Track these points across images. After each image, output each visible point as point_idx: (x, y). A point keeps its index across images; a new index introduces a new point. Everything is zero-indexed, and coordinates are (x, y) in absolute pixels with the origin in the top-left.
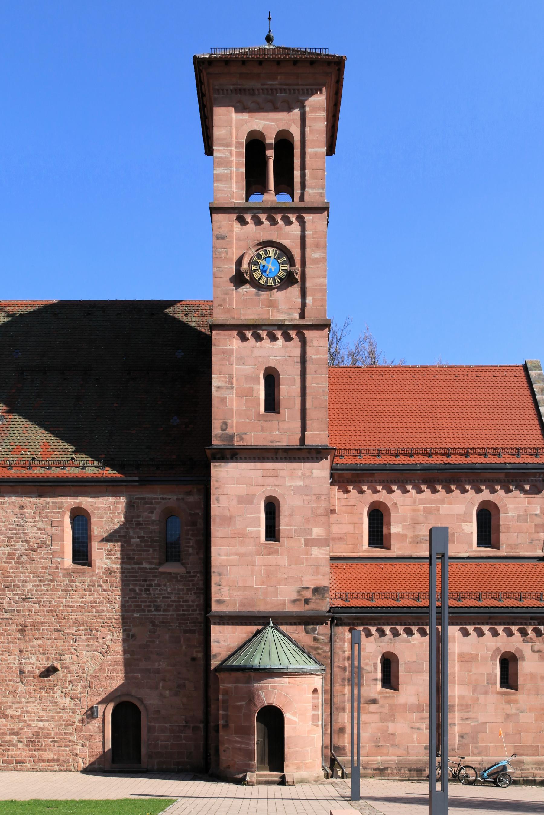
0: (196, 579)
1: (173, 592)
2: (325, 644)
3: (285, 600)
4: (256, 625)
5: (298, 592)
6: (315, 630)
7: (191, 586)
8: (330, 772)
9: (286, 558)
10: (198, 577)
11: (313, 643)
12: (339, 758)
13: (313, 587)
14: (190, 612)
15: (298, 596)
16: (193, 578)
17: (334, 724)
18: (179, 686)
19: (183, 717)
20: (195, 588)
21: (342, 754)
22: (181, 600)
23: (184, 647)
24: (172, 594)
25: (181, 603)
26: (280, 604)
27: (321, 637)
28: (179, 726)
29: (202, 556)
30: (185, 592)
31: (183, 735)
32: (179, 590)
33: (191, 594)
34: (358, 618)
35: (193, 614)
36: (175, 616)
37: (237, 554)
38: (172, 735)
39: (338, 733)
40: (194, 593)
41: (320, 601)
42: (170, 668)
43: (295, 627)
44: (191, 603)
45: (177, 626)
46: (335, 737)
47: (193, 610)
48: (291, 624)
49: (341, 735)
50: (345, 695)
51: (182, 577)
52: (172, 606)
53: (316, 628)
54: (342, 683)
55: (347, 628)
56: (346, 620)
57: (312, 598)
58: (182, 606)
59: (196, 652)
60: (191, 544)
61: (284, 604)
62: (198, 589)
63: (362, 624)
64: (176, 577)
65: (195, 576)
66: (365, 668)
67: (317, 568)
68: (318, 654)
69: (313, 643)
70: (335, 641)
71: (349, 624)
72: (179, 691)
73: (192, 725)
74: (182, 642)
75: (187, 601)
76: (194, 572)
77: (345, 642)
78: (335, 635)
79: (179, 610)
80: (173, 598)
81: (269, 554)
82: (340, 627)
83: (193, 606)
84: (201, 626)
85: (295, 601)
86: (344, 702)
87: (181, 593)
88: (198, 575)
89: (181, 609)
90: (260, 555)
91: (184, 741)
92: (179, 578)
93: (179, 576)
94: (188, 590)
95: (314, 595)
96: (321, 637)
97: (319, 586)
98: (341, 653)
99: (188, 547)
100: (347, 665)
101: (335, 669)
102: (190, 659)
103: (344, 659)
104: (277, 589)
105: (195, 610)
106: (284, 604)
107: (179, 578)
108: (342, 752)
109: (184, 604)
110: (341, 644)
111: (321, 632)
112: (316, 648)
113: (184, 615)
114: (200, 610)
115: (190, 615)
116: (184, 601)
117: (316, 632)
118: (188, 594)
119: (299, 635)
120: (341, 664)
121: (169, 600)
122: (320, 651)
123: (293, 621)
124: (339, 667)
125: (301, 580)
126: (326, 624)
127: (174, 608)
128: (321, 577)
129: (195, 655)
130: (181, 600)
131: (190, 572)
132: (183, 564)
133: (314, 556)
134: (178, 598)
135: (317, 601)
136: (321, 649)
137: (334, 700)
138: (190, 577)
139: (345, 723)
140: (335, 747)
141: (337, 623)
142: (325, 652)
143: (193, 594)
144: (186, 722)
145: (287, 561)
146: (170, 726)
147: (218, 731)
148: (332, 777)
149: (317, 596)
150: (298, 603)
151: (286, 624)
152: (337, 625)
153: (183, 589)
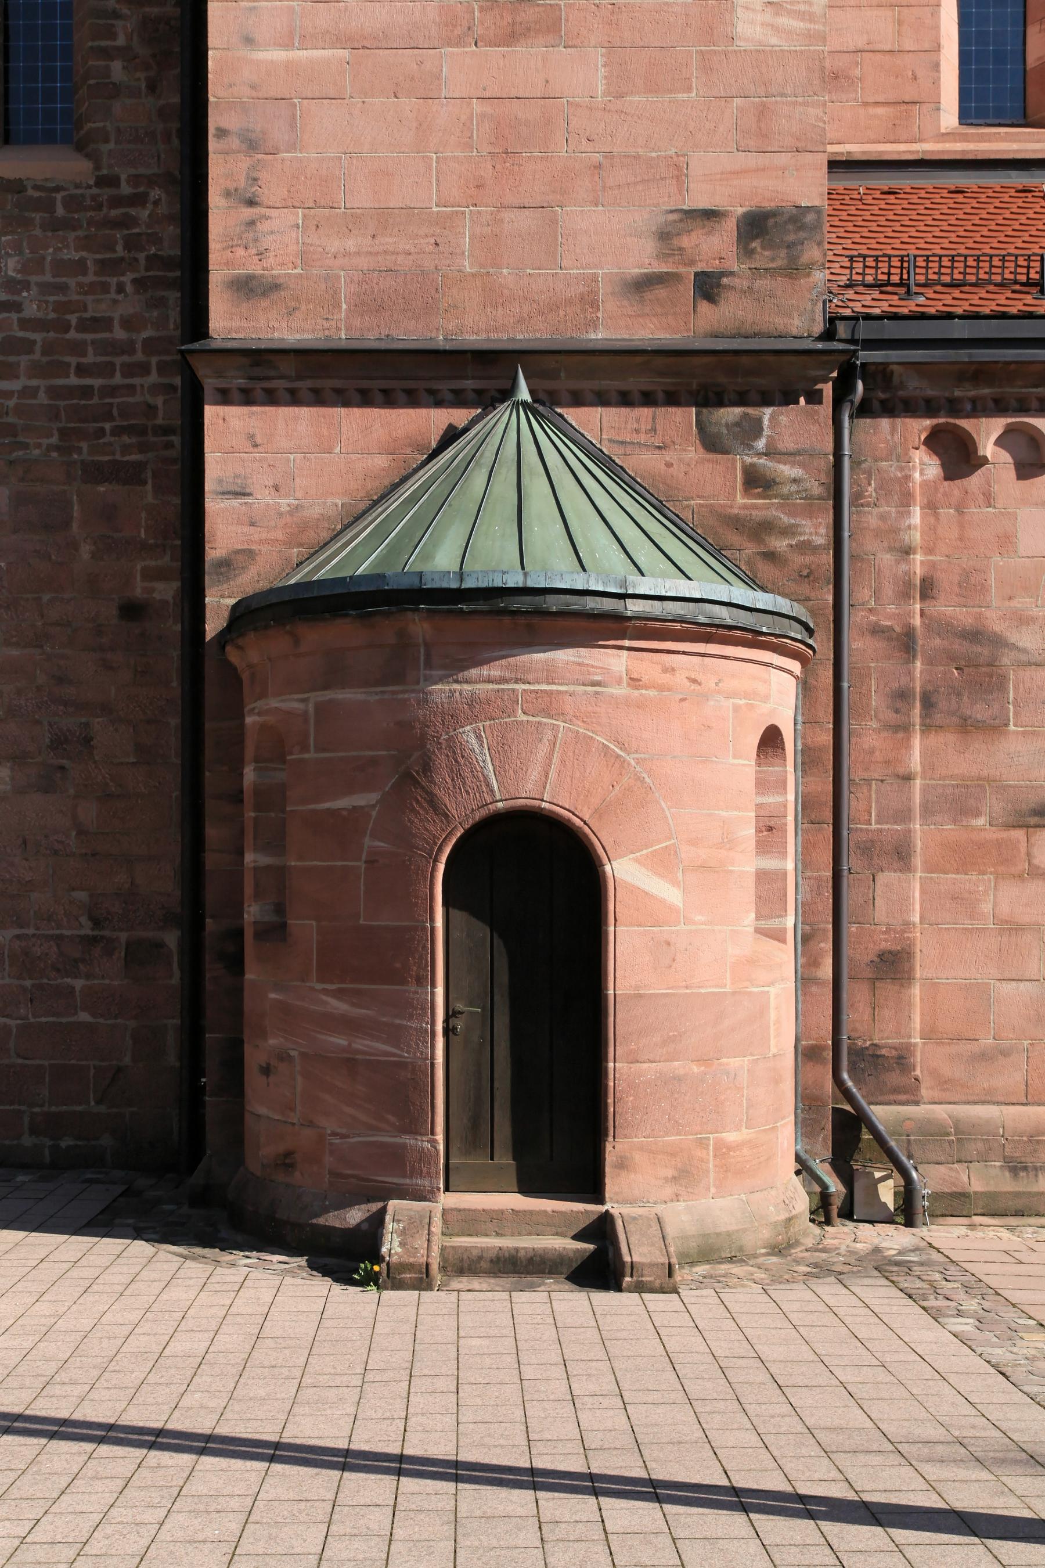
0: (144, 214)
1: (34, 279)
2: (809, 510)
3: (595, 278)
4: (439, 404)
5: (664, 236)
6: (753, 429)
7: (120, 251)
8: (835, 1186)
9: (599, 57)
10: (156, 203)
11: (741, 501)
12: (880, 1114)
13: (741, 211)
14: (118, 379)
15: (661, 256)
16: (133, 212)
17: (849, 929)
18: (59, 743)
19: (82, 896)
20: (142, 256)
21: (896, 1090)
22: (73, 319)
23: (86, 550)
24: (26, 285)
25: (72, 334)
26: (570, 302)
27: (787, 470)
28: (60, 938)
29: (176, 100)
30: (91, 278)
31: (78, 984)
32: (61, 267)
33: (120, 289)
34: (979, 374)
35: (131, 389)
36: (43, 398)
37: (340, 40)
38: (28, 983)
39: (873, 981)
40: (134, 281)
41: (779, 284)
42: (15, 652)
43: (646, 412)
44: (119, 334)
45: (50, 448)
46: (856, 995)
47: (130, 370)
48: (625, 400)
49: (886, 988)
50: (908, 778)
51: (73, 203)
52: (28, 346)
53: (759, 421)
54: (890, 716)
55: (920, 427)
56: (915, 386)
57: (736, 269)
58: (78, 348)
59: (150, 575)
60: (121, 41)
61: (590, 301)
62: (153, 261)
63: (999, 407)
64: (48, 206)
65: (138, 200)
66: (1013, 637)
67: (762, 111)
68: (771, 556)
69: (741, 501)
70: (857, 497)
71: (929, 408)
72: (62, 768)
73: (123, 936)
74: (75, 526)
75: (102, 323)
76: (134, 180)
77: (906, 500)
78: (856, 464)
79: (60, 369)
80: (31, 310)
81: (511, 37)
82: (885, 423)
83: (128, 348)
84: (169, 445)
85: (644, 284)
86: (904, 815)
87: (72, 282)
88: (155, 193)
89: (73, 361)
90: (459, 42)
91: (84, 1017)
92: (60, 211)
93: (59, 196)
94: (108, 266)
95: (748, 253)
96: (787, 470)
97: (769, 205)
98: (886, 558)
99: (106, 54)
100: (917, 621)
101: (855, 643)
102: (115, 612)
103: (904, 594)
104: (554, 221)
105: (144, 369)
106: (590, 301)
107: (60, 211)
108: (894, 1078)
109: (89, 337)
110: (889, 509)
111: (787, 443)
112: (762, 529)
113: (86, 392)
114: (162, 368)
115: (112, 391)
116: (84, 326)
117: (761, 444)
118: (105, 288)
119: (669, 456)
120: (889, 614)
121: (14, 316)
122: (780, 544)
123: (635, 384)
124: (876, 631)
125: (680, 174)
126: (814, 398)
127: (37, 356)
128: (783, 159)
129: (138, 590)
130: (73, 319)
131: (111, 181)
132: (80, 147)
133: (742, 45)
134: (63, 307)
135: (763, 284)
136: (787, 531)
137: (854, 804)
138: (117, 202)
139: (908, 925)
140: (857, 1053)
141: (864, 401)
142: (805, 547)
143: (129, 288)
144: (97, 923)
145: (602, 72)
146: (18, 937)
147: (236, 964)
148: (848, 1213)
149: (763, 257)
150: (661, 292)
151: (602, 400)
152: (864, 410)
153: (80, 266)
